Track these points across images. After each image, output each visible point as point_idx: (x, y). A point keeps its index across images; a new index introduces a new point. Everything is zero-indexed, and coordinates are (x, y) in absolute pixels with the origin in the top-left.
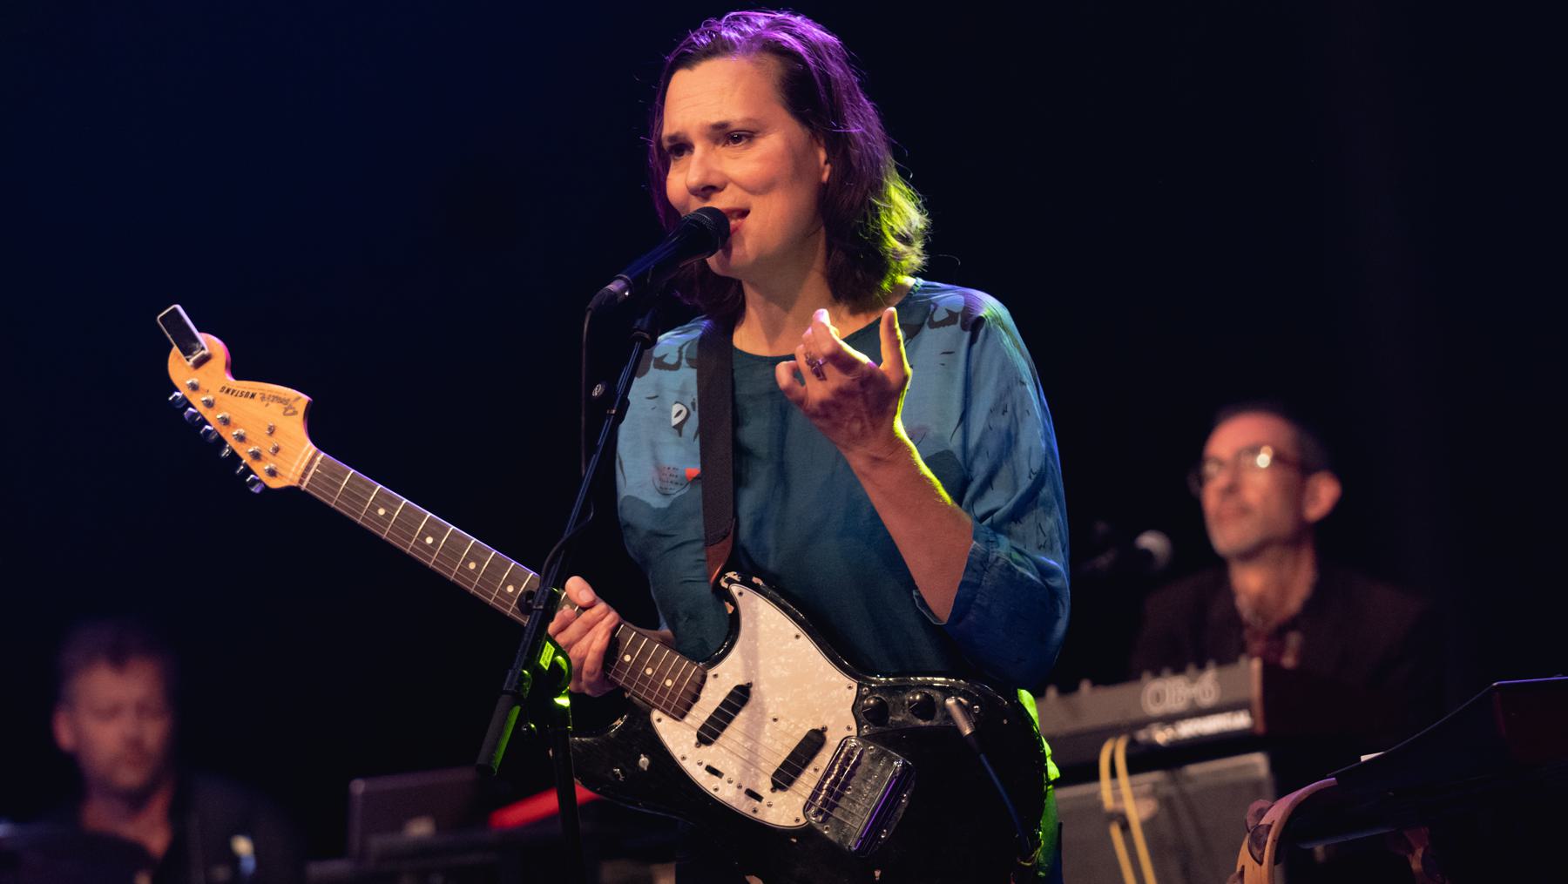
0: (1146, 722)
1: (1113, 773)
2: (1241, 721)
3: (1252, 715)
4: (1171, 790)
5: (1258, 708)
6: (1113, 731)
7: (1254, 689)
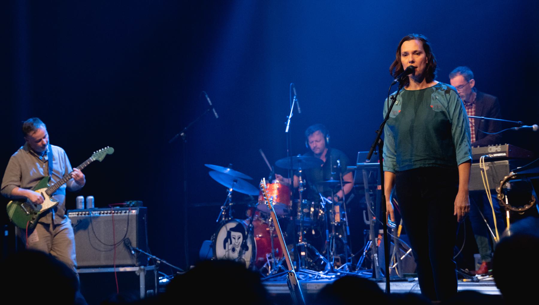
0: (488, 154)
1: (482, 162)
2: (504, 154)
3: (506, 154)
4: (492, 165)
5: (507, 153)
6: (483, 155)
7: (507, 150)
